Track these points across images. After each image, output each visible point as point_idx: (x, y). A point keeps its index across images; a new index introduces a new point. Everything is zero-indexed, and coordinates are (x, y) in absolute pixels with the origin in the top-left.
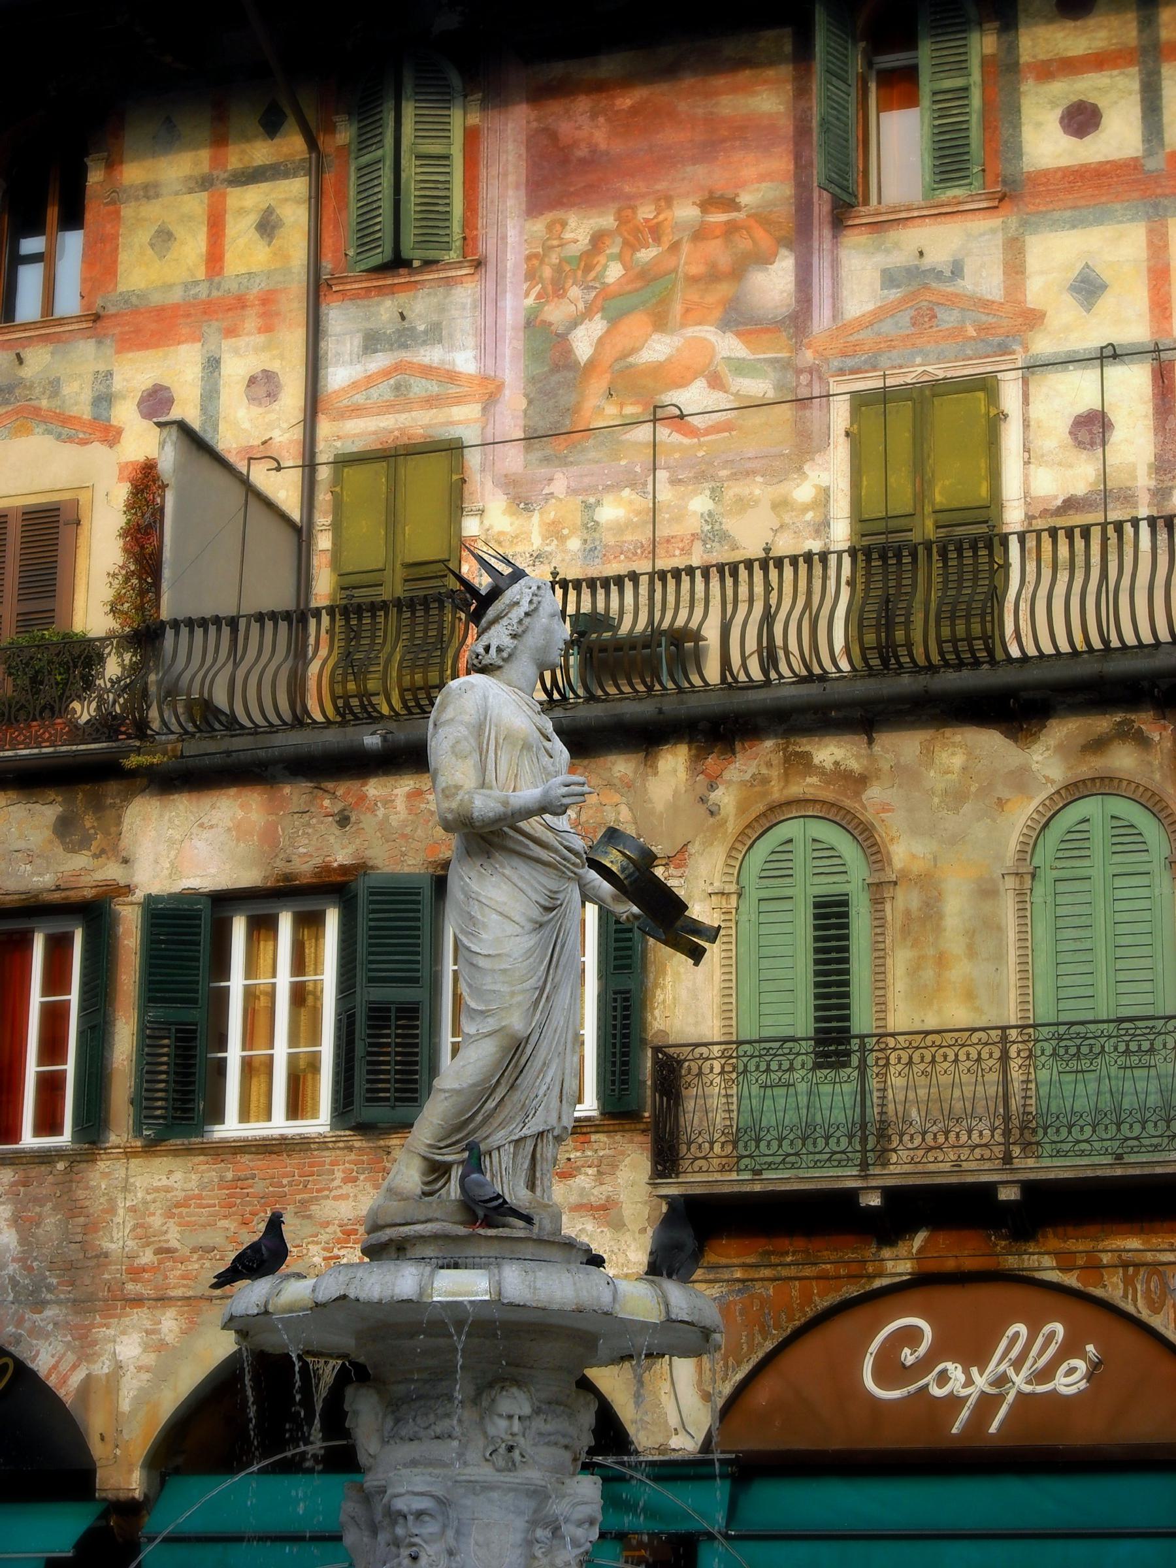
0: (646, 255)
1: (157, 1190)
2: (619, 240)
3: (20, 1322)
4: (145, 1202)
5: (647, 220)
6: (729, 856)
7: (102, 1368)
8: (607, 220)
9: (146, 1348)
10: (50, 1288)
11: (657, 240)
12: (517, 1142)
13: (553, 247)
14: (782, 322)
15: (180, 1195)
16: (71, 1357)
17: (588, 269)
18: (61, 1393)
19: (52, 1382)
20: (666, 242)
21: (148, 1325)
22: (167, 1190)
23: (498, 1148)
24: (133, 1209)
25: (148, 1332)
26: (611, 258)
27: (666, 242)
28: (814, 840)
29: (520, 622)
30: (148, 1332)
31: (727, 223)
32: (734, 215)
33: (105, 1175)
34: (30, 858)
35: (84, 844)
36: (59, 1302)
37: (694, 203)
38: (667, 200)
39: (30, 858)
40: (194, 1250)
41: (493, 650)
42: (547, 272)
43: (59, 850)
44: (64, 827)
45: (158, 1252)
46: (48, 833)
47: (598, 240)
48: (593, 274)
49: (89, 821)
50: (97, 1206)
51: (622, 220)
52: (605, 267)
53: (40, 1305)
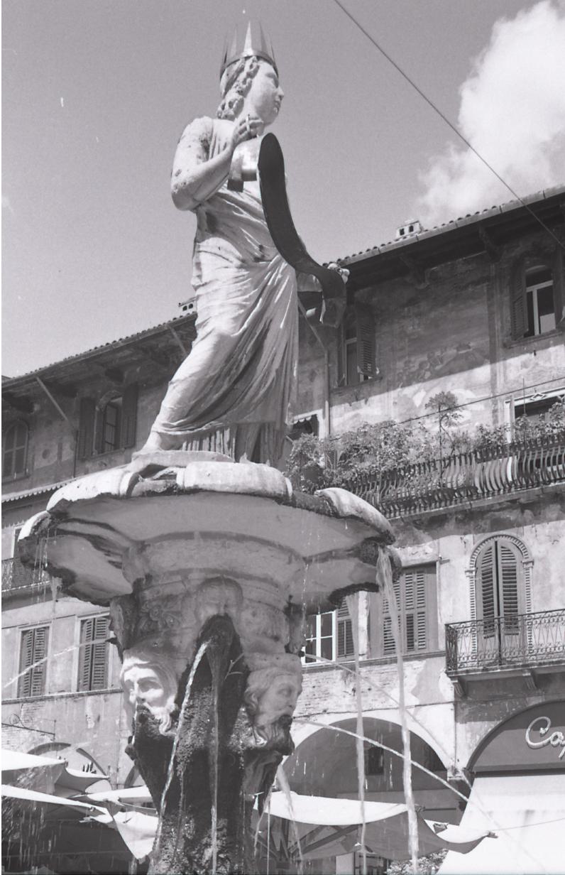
0: (438, 368)
2: (429, 364)
5: (438, 356)
6: (472, 558)
8: (425, 358)
11: (442, 362)
13: (406, 370)
14: (486, 384)
17: (419, 375)
20: (445, 362)
26: (426, 370)
27: (445, 362)
28: (502, 547)
29: (244, 82)
31: (465, 353)
32: (468, 350)
37: (454, 349)
38: (446, 348)
41: (227, 107)
42: (405, 378)
47: (421, 365)
48: (420, 377)
51: (429, 357)
52: (424, 374)
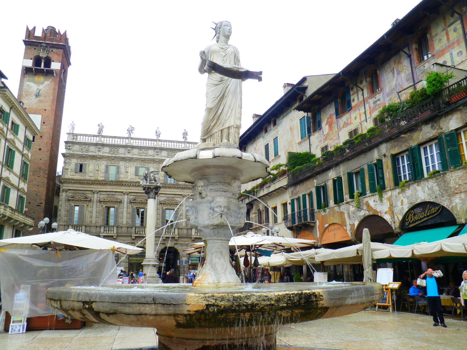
1: (456, 176)
3: (441, 200)
4: (455, 178)
7: (454, 204)
9: (460, 200)
10: (444, 194)
12: (222, 131)
15: (460, 176)
16: (449, 203)
18: (449, 209)
19: (447, 208)
21: (459, 196)
22: (458, 175)
23: (216, 133)
24: (453, 180)
25: (460, 198)
30: (460, 198)
33: (448, 175)
34: (428, 133)
35: (435, 128)
36: (446, 196)
39: (428, 133)
40: (464, 184)
43: (432, 130)
44: (432, 127)
45: (459, 185)
46: (430, 128)
49: (435, 125)
50: (448, 180)
53: (443, 197)
